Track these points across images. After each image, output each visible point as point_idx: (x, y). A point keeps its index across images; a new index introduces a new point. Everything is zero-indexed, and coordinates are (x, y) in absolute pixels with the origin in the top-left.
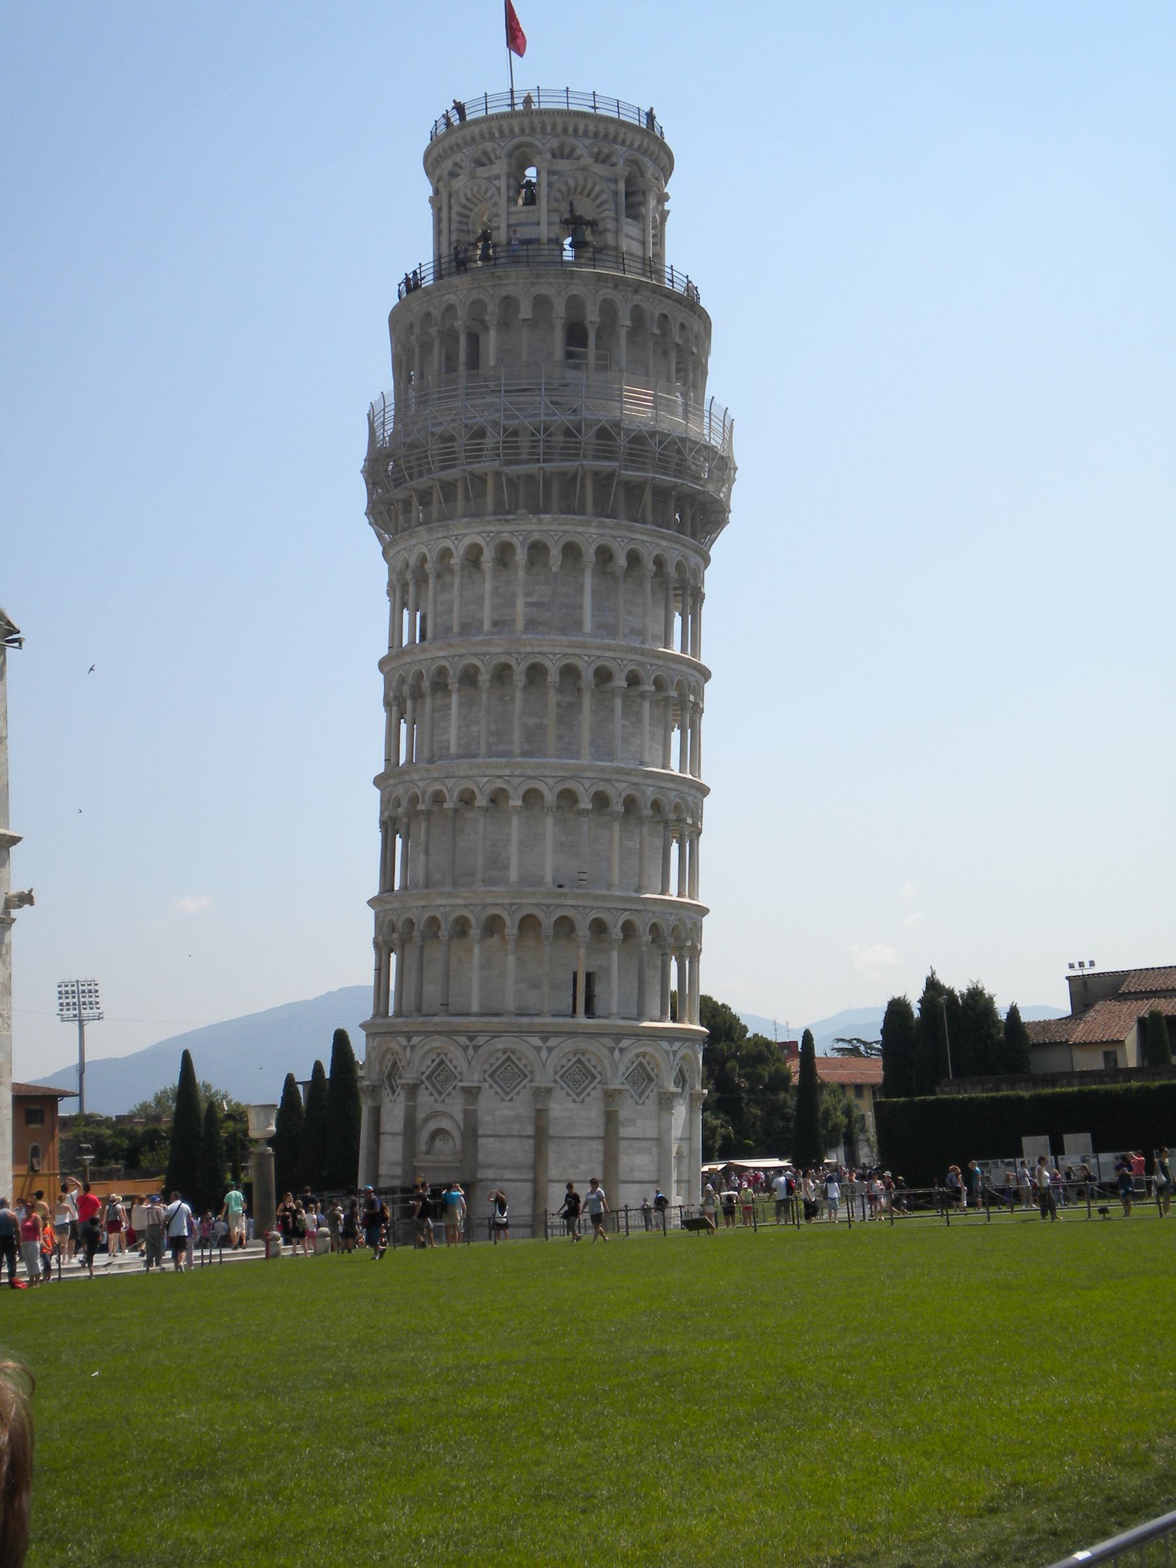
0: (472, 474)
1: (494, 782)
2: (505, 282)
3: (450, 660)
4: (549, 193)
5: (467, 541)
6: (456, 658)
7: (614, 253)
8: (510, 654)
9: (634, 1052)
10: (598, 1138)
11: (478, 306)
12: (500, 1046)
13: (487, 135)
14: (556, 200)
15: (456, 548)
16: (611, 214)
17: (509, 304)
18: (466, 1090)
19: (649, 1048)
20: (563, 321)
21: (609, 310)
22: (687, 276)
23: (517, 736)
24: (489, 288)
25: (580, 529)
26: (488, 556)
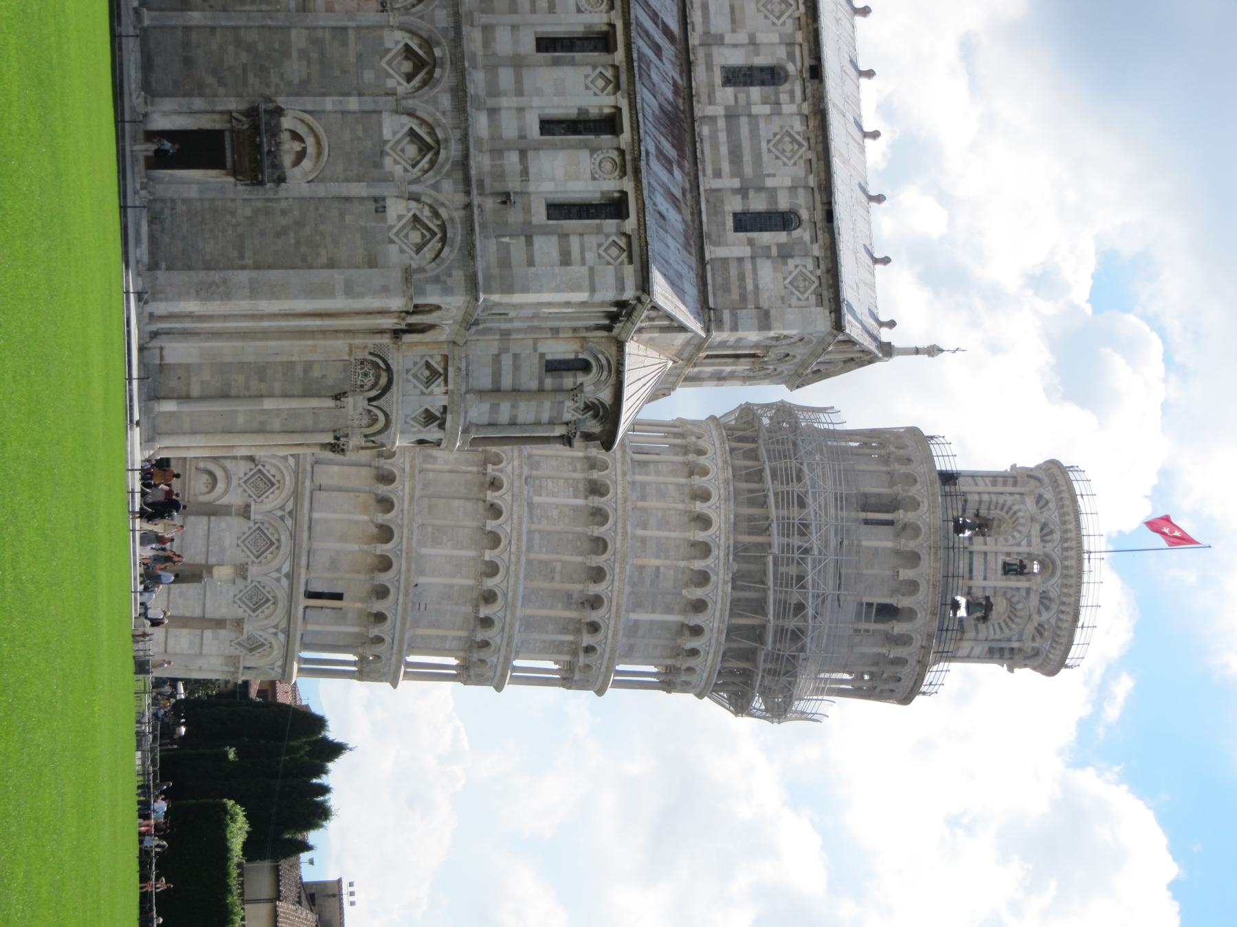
0: (770, 525)
1: (506, 537)
2: (932, 558)
3: (614, 500)
4: (1011, 588)
5: (714, 517)
6: (614, 506)
7: (958, 638)
8: (614, 554)
9: (273, 641)
10: (204, 613)
11: (916, 531)
12: (283, 538)
13: (1065, 536)
14: (1005, 593)
15: (709, 507)
16: (991, 637)
17: (913, 558)
18: (248, 506)
19: (277, 652)
20: (895, 605)
21: (904, 640)
22: (936, 692)
23: (544, 556)
24: (928, 543)
25: (717, 614)
26: (701, 536)
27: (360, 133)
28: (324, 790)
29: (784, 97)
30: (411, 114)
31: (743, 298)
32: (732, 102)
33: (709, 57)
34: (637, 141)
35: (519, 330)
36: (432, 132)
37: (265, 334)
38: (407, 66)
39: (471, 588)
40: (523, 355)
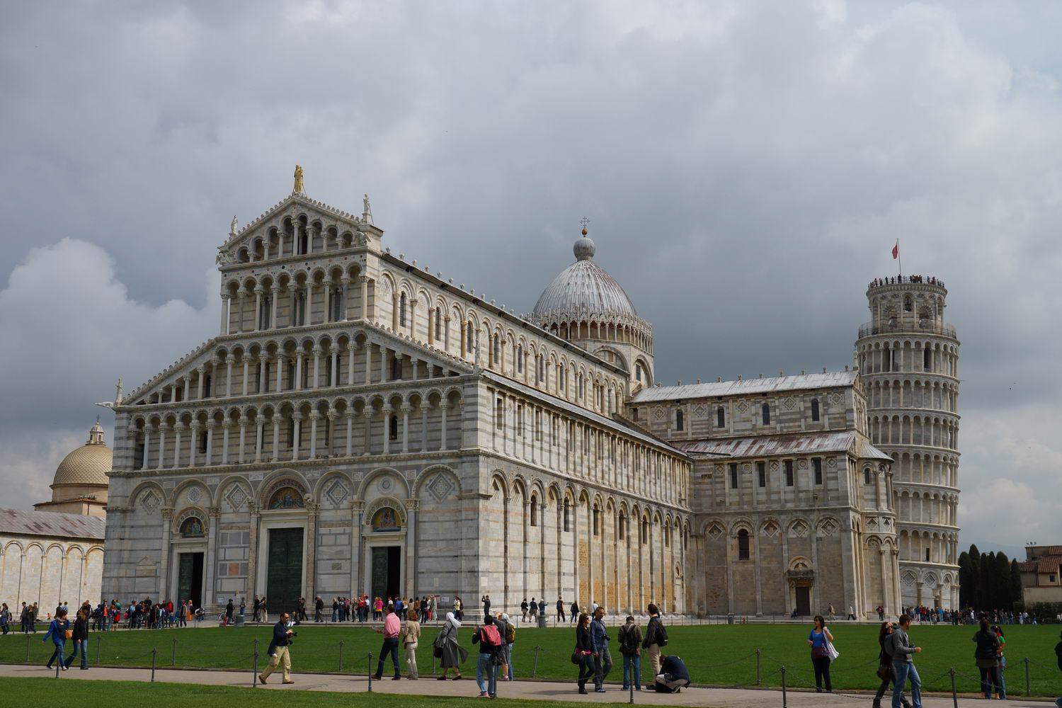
5: (893, 415)
17: (907, 344)
21: (937, 346)
26: (901, 419)
27: (794, 545)
28: (992, 553)
29: (773, 404)
30: (788, 528)
31: (842, 418)
32: (775, 422)
33: (760, 429)
34: (794, 454)
35: (857, 493)
36: (794, 522)
37: (862, 577)
38: (771, 529)
39: (923, 501)
40: (864, 491)
